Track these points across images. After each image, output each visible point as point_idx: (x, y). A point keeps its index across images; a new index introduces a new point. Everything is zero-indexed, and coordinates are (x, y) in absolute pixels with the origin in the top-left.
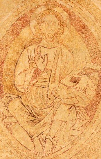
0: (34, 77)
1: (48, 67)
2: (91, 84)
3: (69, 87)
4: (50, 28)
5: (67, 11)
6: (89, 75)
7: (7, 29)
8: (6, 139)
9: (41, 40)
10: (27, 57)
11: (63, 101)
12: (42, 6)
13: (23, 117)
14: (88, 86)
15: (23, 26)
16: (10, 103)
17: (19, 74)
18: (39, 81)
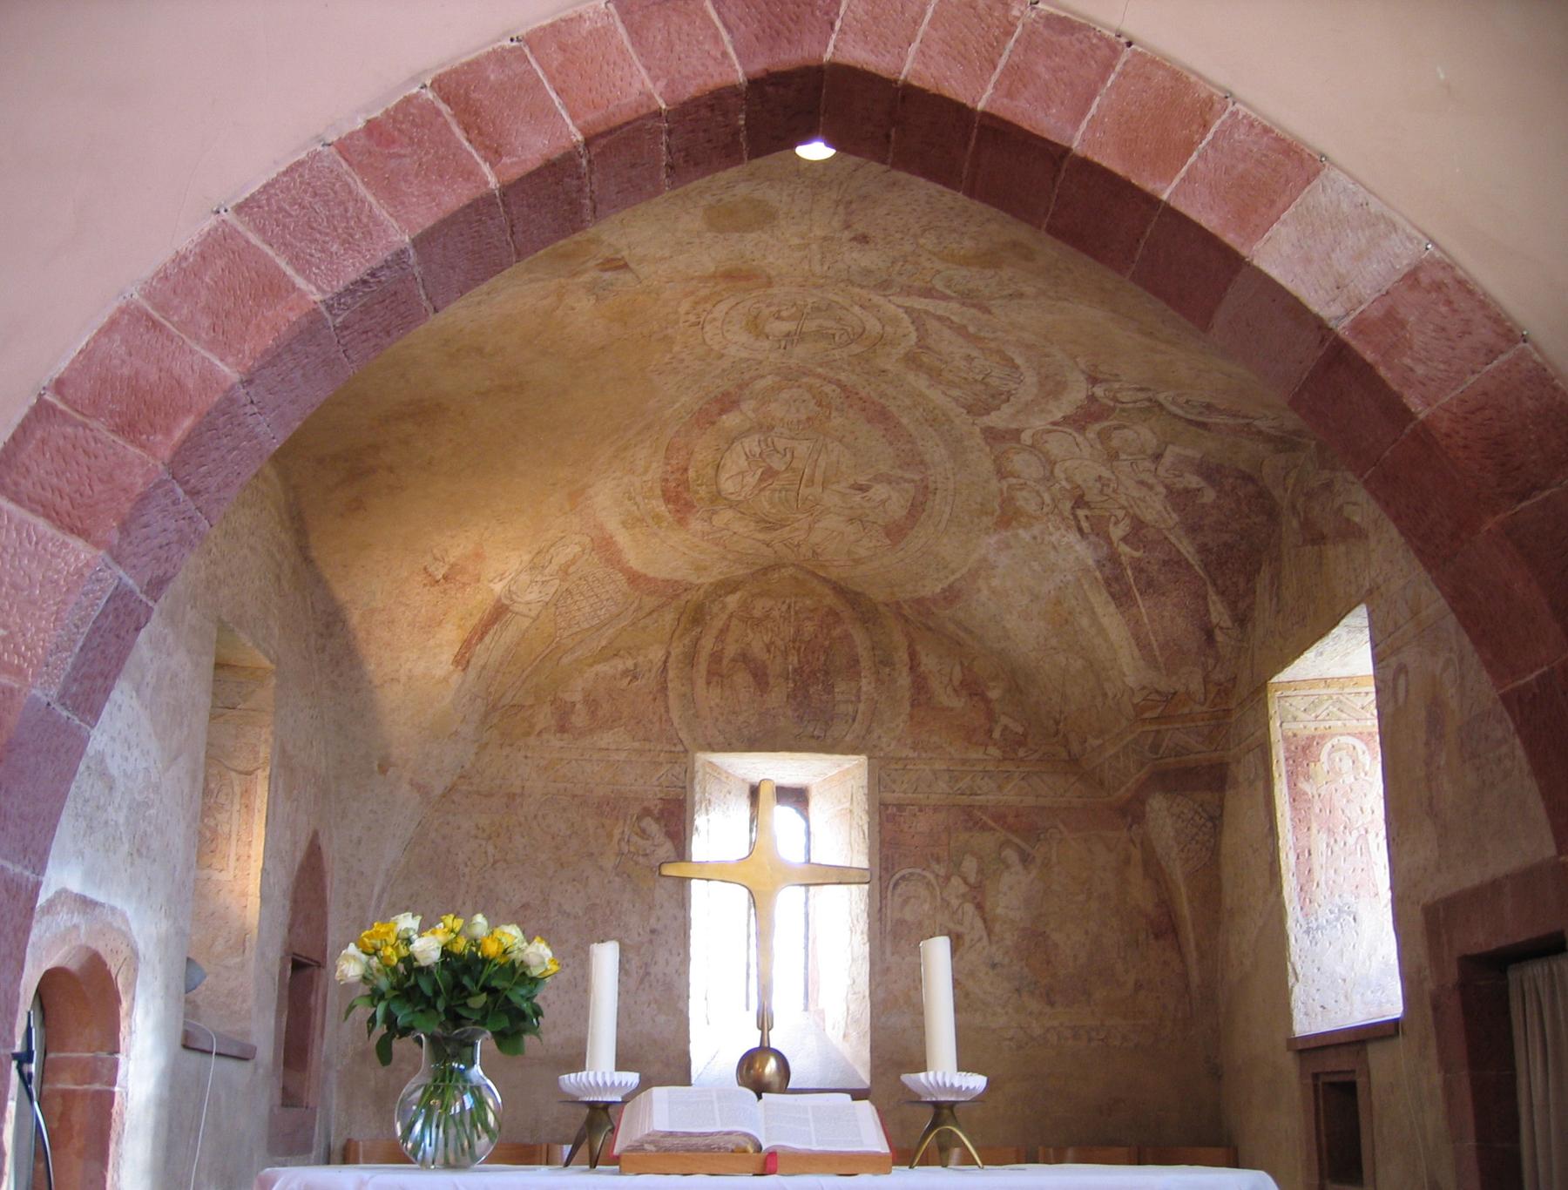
0: (761, 480)
1: (794, 465)
2: (895, 495)
3: (843, 495)
4: (793, 410)
5: (839, 383)
6: (894, 484)
7: (683, 420)
8: (716, 556)
9: (771, 428)
10: (743, 454)
11: (832, 509)
12: (769, 377)
13: (746, 526)
14: (889, 498)
15: (723, 411)
16: (714, 516)
17: (727, 479)
18: (776, 482)
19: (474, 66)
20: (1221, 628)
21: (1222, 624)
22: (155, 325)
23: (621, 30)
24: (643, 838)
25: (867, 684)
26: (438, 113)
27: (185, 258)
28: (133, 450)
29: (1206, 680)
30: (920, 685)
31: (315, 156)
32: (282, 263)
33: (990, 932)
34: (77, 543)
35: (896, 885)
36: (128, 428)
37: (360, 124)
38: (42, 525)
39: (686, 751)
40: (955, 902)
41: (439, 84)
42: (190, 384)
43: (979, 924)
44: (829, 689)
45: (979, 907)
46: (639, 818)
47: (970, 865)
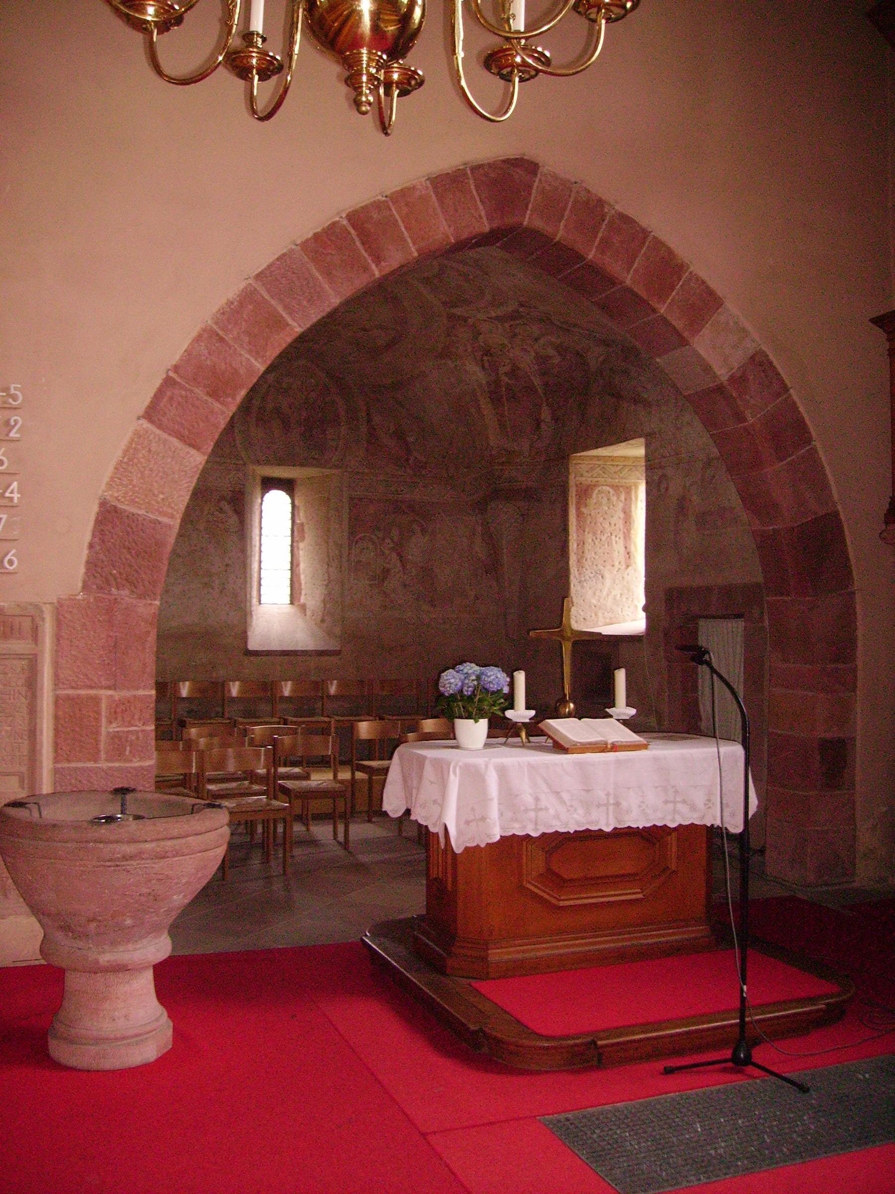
19: (365, 209)
20: (545, 422)
21: (546, 420)
22: (221, 340)
23: (434, 198)
24: (221, 513)
25: (343, 430)
26: (349, 233)
27: (232, 303)
28: (217, 405)
29: (531, 446)
30: (372, 433)
31: (292, 251)
32: (280, 309)
33: (404, 567)
34: (193, 452)
35: (357, 542)
36: (214, 394)
37: (310, 235)
38: (176, 442)
39: (245, 465)
40: (387, 552)
41: (349, 217)
42: (242, 371)
43: (399, 564)
44: (324, 432)
45: (399, 554)
46: (219, 501)
47: (395, 533)
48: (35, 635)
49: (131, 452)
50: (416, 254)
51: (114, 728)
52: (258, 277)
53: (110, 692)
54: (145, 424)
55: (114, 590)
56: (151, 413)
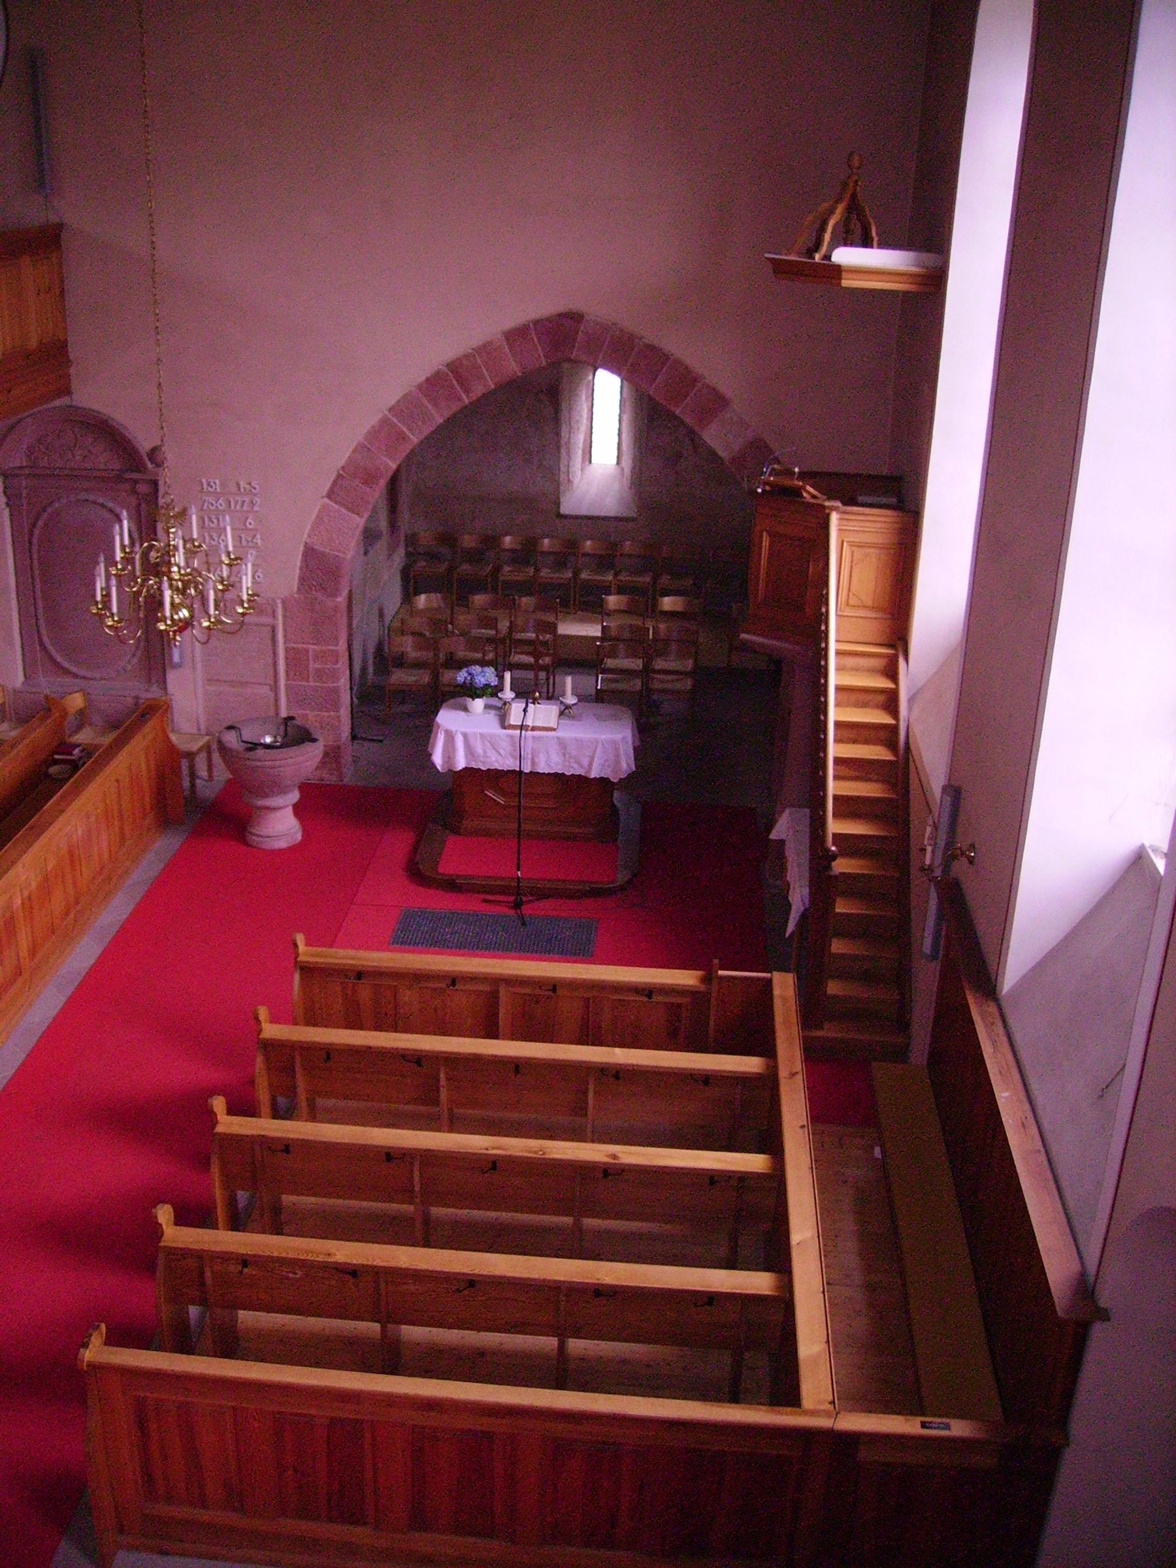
19: (459, 360)
37: (424, 378)
38: (344, 511)
48: (274, 615)
49: (319, 520)
50: (493, 387)
51: (317, 666)
52: (390, 410)
53: (315, 647)
54: (327, 501)
55: (314, 593)
56: (330, 495)
